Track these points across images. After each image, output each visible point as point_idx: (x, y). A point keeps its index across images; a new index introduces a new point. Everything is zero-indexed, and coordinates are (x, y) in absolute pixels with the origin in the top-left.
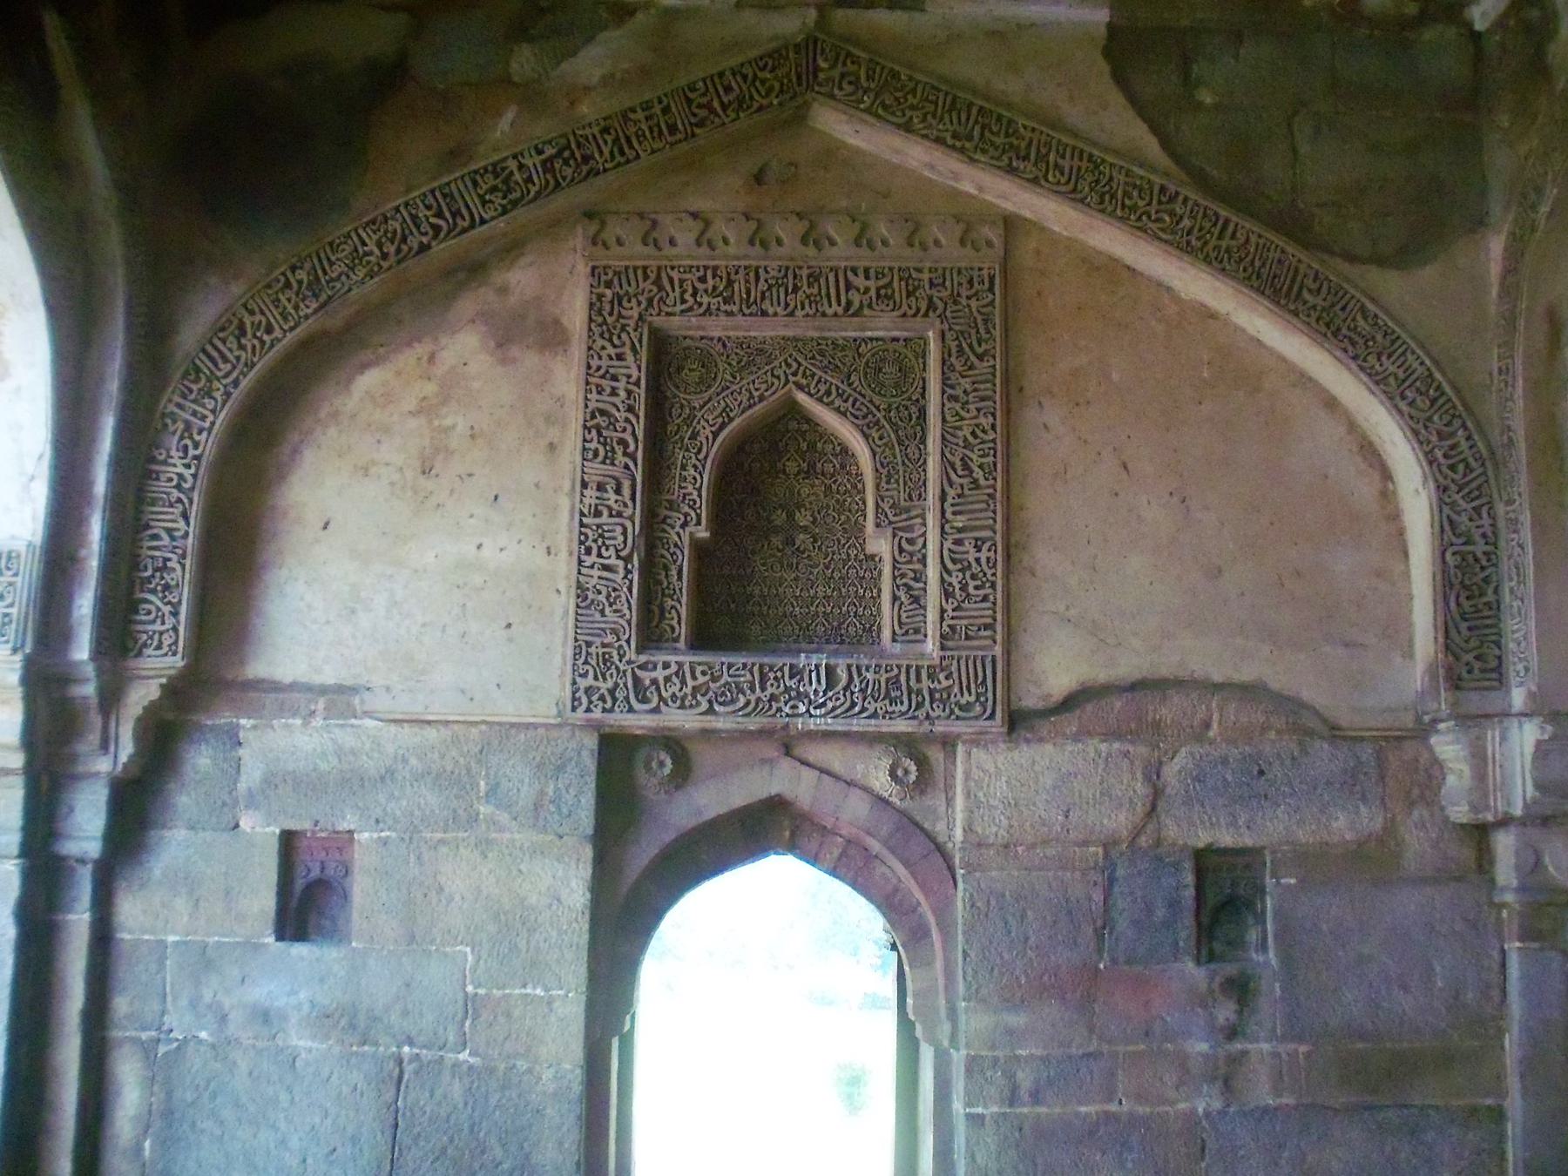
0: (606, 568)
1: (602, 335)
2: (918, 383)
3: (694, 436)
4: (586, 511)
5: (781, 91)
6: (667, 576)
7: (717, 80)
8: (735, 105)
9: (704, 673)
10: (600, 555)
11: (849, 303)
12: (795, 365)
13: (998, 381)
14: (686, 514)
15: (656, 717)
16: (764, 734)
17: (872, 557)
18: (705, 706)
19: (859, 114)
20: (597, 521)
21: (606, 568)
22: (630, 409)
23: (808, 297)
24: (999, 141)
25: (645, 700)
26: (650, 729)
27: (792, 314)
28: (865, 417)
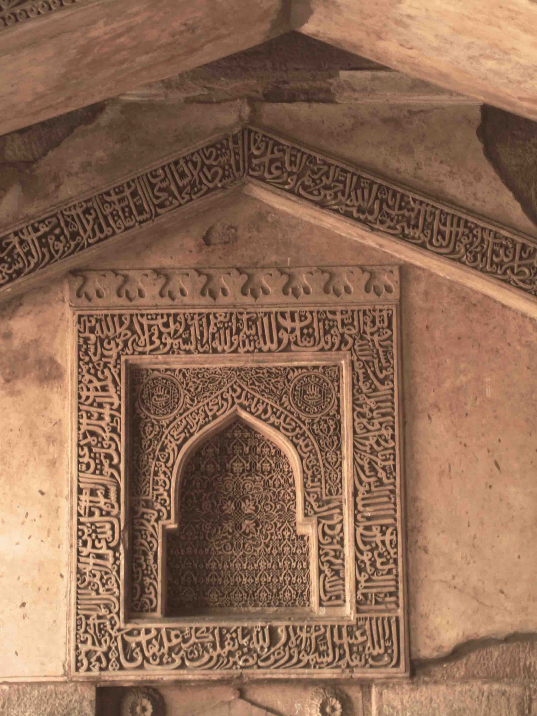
1: (88, 372)
2: (334, 401)
3: (163, 449)
4: (82, 512)
5: (224, 177)
7: (173, 167)
8: (189, 188)
9: (177, 636)
10: (94, 547)
11: (280, 342)
12: (239, 390)
13: (396, 400)
15: (140, 672)
16: (222, 682)
19: (284, 193)
20: (91, 519)
21: (99, 556)
23: (248, 337)
24: (394, 213)
25: (132, 659)
26: (135, 681)
27: (235, 351)
28: (293, 430)
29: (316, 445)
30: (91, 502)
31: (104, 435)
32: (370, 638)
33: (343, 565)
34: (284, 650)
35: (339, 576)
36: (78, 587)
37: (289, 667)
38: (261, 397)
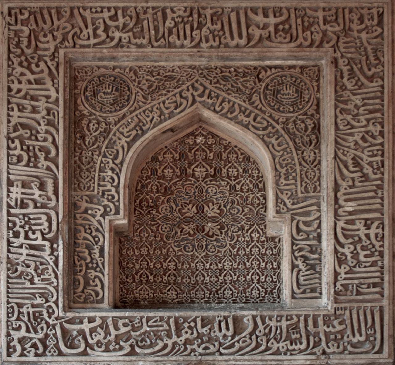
0: (32, 247)
4: (13, 204)
6: (90, 254)
12: (201, 89)
14: (105, 207)
17: (273, 239)
18: (128, 349)
22: (49, 123)
25: (72, 347)
29: (291, 144)
30: (22, 193)
31: (39, 128)
32: (349, 326)
33: (320, 260)
34: (250, 339)
35: (315, 270)
36: (8, 277)
37: (257, 354)
38: (226, 96)
